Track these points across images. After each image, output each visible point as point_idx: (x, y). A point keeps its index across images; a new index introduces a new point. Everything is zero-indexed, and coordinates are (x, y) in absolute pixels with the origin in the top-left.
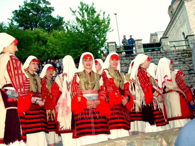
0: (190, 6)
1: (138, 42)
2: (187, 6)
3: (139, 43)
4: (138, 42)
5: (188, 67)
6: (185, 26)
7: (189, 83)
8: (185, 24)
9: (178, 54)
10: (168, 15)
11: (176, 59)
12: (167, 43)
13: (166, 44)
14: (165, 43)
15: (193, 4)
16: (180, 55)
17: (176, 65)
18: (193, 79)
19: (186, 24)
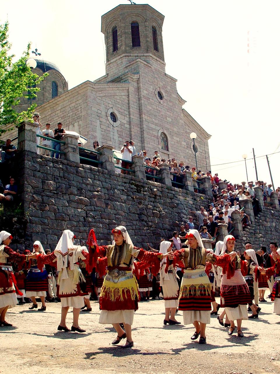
0: (95, 99)
1: (72, 141)
2: (90, 97)
3: (73, 144)
4: (72, 141)
6: (74, 126)
7: (140, 236)
8: (76, 124)
9: (125, 183)
13: (110, 160)
15: (98, 98)
19: (79, 125)
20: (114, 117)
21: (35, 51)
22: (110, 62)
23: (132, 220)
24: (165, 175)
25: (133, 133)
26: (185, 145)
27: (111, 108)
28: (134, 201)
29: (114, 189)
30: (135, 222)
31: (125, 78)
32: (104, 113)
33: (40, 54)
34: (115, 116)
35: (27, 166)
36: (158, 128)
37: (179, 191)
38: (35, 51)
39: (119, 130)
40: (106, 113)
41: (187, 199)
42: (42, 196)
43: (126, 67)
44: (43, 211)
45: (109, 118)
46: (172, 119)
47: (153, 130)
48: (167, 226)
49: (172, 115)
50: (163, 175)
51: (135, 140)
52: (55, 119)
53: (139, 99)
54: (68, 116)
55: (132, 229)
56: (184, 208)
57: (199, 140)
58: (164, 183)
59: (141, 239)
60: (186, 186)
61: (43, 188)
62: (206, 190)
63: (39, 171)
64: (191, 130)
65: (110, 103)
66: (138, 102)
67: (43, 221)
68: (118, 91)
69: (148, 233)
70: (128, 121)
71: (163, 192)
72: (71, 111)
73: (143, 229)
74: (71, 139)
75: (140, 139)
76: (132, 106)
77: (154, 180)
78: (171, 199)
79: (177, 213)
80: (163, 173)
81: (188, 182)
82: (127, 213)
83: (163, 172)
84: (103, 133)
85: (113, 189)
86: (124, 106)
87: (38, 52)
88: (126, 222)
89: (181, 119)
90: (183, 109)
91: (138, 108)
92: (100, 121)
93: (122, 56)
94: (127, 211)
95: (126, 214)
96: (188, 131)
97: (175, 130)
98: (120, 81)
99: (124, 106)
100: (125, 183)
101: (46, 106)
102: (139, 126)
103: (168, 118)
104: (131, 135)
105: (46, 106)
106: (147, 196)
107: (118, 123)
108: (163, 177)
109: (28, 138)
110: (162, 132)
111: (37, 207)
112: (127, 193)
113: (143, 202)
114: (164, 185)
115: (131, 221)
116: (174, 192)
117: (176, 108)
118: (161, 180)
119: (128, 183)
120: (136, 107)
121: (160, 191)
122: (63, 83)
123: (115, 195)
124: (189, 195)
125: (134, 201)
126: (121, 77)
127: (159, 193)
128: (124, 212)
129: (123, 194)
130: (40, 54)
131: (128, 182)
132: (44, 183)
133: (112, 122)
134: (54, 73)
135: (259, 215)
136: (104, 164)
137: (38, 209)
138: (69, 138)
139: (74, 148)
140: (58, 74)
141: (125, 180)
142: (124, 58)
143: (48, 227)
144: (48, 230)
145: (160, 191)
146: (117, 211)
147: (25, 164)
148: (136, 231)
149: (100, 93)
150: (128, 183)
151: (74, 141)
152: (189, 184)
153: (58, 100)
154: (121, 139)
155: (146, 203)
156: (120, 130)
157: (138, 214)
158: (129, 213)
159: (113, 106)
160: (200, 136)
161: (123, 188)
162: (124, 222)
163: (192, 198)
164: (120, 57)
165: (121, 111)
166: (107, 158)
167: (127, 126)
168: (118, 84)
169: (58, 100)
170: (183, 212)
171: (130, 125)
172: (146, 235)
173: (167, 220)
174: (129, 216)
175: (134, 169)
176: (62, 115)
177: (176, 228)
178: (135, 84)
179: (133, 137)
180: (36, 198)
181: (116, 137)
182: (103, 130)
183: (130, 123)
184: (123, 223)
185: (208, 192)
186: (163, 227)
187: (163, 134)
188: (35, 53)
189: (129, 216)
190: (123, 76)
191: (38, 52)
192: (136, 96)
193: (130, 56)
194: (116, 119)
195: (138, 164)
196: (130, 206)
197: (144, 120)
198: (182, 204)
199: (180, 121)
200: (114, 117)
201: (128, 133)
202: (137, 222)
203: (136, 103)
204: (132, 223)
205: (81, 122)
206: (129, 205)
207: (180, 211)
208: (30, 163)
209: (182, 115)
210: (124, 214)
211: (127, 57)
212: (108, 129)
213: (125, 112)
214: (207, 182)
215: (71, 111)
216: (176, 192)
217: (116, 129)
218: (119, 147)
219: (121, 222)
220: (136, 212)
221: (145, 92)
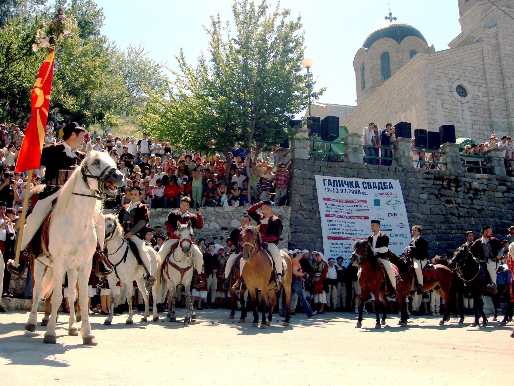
1: (353, 140)
3: (355, 143)
4: (353, 140)
5: (444, 209)
6: (411, 111)
7: (445, 241)
10: (353, 69)
11: (424, 188)
12: (409, 152)
13: (407, 154)
14: (404, 152)
15: (438, 70)
16: (431, 182)
17: (423, 201)
18: (452, 234)
19: (416, 109)
20: (462, 91)
21: (388, 16)
22: (463, 17)
24: (495, 163)
25: (492, 107)
27: (457, 80)
28: (440, 200)
29: (409, 188)
30: (437, 225)
31: (478, 35)
32: (446, 89)
33: (395, 19)
34: (464, 89)
35: (296, 175)
38: (388, 16)
39: (470, 106)
40: (450, 87)
42: (312, 204)
43: (482, 19)
44: (312, 219)
45: (455, 94)
50: (493, 163)
51: (497, 116)
52: (393, 104)
53: (500, 59)
54: (405, 98)
55: (433, 234)
58: (493, 173)
61: (313, 196)
63: (310, 179)
65: (456, 73)
66: (499, 64)
67: (312, 230)
68: (467, 56)
69: (458, 237)
70: (485, 91)
71: (490, 185)
72: (407, 92)
73: (450, 233)
74: (352, 138)
75: (505, 113)
76: (490, 71)
77: (475, 171)
80: (493, 160)
82: (427, 215)
83: (492, 159)
84: (447, 113)
85: (408, 188)
86: (478, 73)
87: (393, 16)
88: (424, 225)
91: (499, 72)
92: (442, 100)
93: (475, 6)
94: (428, 212)
95: (426, 216)
98: (472, 40)
99: (478, 73)
100: (428, 179)
101: (382, 91)
102: (503, 96)
104: (490, 110)
105: (382, 91)
107: (469, 97)
108: (493, 166)
109: (298, 146)
111: (305, 216)
113: (453, 199)
115: (433, 224)
116: (509, 184)
118: (490, 171)
119: (431, 179)
120: (495, 71)
121: (485, 184)
122: (425, 50)
123: (411, 195)
125: (440, 200)
126: (472, 35)
128: (422, 214)
130: (395, 19)
131: (433, 177)
132: (315, 190)
133: (460, 98)
134: (412, 40)
136: (399, 160)
137: (306, 217)
138: (349, 137)
139: (356, 148)
140: (418, 40)
141: (429, 176)
142: (478, 7)
143: (317, 236)
144: (316, 238)
145: (485, 184)
147: (294, 173)
148: (439, 235)
149: (438, 64)
150: (431, 179)
151: (356, 139)
153: (393, 81)
154: (474, 118)
155: (459, 201)
156: (472, 105)
157: (444, 215)
158: (431, 214)
159: (460, 76)
161: (424, 186)
164: (473, 8)
165: (473, 81)
166: (401, 152)
167: (485, 99)
168: (465, 47)
169: (393, 81)
171: (488, 97)
172: (455, 239)
174: (429, 218)
176: (399, 99)
178: (493, 41)
179: (493, 112)
180: (305, 207)
181: (467, 115)
182: (447, 110)
183: (487, 94)
188: (388, 18)
190: (474, 34)
191: (393, 16)
192: (496, 57)
193: (486, 3)
194: (466, 93)
197: (508, 86)
200: (462, 91)
201: (486, 107)
202: (441, 224)
203: (496, 65)
205: (417, 105)
208: (299, 171)
210: (421, 216)
211: (482, 6)
212: (455, 107)
213: (480, 81)
215: (407, 92)
217: (466, 105)
218: (472, 128)
220: (440, 213)
221: (509, 48)
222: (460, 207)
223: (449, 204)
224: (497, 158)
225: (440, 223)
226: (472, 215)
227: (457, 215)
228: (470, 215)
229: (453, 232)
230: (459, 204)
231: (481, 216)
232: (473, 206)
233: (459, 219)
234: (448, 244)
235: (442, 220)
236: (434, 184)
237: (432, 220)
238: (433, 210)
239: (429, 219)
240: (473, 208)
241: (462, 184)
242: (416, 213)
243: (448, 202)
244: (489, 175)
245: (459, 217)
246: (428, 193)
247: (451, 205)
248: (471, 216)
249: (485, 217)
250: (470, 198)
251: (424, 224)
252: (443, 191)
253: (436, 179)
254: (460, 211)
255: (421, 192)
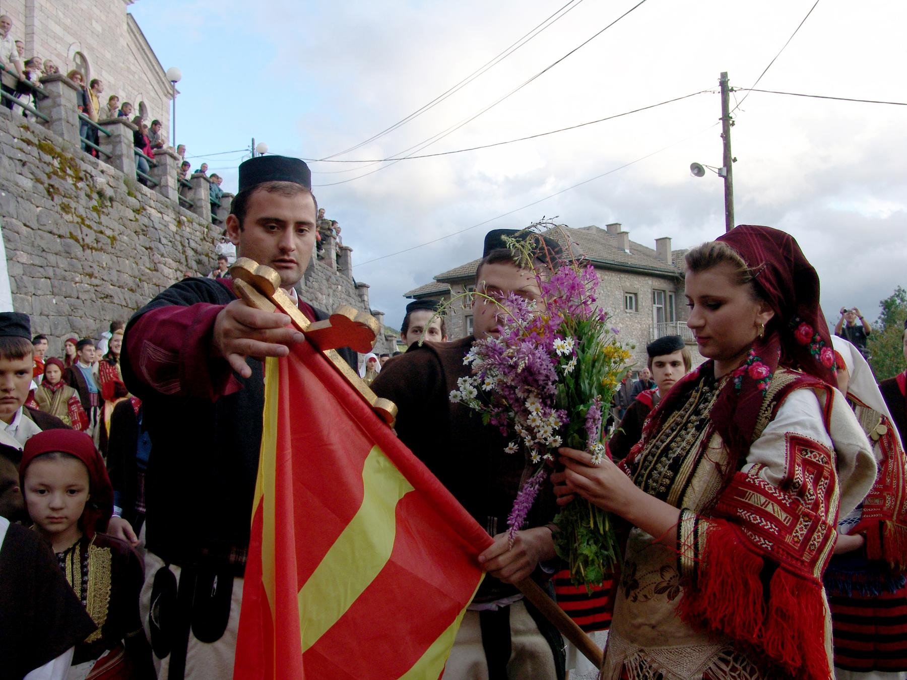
9: (29, 143)
23: (44, 251)
26: (125, 97)
28: (53, 200)
30: (52, 258)
36: (70, 39)
37: (149, 195)
41: (166, 217)
46: (103, 29)
47: (57, 40)
48: (126, 278)
49: (104, 18)
50: (118, 148)
55: (46, 278)
56: (160, 239)
57: (153, 94)
58: (120, 168)
59: (67, 307)
60: (161, 187)
62: (198, 204)
64: (140, 68)
73: (73, 280)
78: (137, 211)
79: (147, 249)
80: (120, 142)
81: (169, 179)
89: (122, 35)
90: (128, 14)
96: (132, 68)
97: (108, 56)
100: (29, 143)
103: (94, 23)
106: (82, 194)
108: (118, 152)
110: (78, 53)
112: (32, 173)
113: (73, 205)
114: (121, 174)
115: (44, 253)
117: (116, 5)
124: (170, 211)
125: (53, 200)
127: (109, 192)
128: (25, 225)
129: (20, 174)
135: (310, 278)
141: (28, 135)
146: (5, 219)
148: (56, 283)
152: (170, 184)
155: (82, 211)
157: (60, 236)
158: (39, 229)
160: (155, 87)
162: (25, 255)
163: (174, 217)
170: (158, 249)
173: (127, 262)
175: (51, 112)
177: (145, 284)
184: (22, 256)
185: (204, 211)
186: (118, 280)
187: (78, 57)
189: (38, 238)
195: (63, 101)
196: (41, 211)
198: (156, 229)
199: (121, 40)
202: (58, 257)
204: (46, 259)
206: (37, 207)
207: (152, 245)
209: (125, 27)
214: (202, 185)
216: (144, 197)
219: (18, 253)
220: (55, 231)
222: (84, 224)
223: (67, 213)
224: (126, 141)
225: (56, 254)
226: (103, 247)
227: (81, 241)
228: (100, 245)
229: (77, 279)
230: (80, 217)
231: (113, 251)
232: (103, 229)
233: (84, 250)
234: (70, 305)
235: (59, 248)
236: (40, 160)
237: (43, 244)
238: (44, 220)
239: (38, 241)
240: (101, 232)
241: (82, 174)
242: (14, 220)
243: (65, 208)
244: (117, 171)
245: (84, 247)
246: (31, 176)
247: (68, 217)
248: (101, 249)
249: (119, 254)
250: (95, 209)
251: (29, 248)
252: (55, 181)
253: (40, 147)
254: (84, 233)
255: (18, 171)
